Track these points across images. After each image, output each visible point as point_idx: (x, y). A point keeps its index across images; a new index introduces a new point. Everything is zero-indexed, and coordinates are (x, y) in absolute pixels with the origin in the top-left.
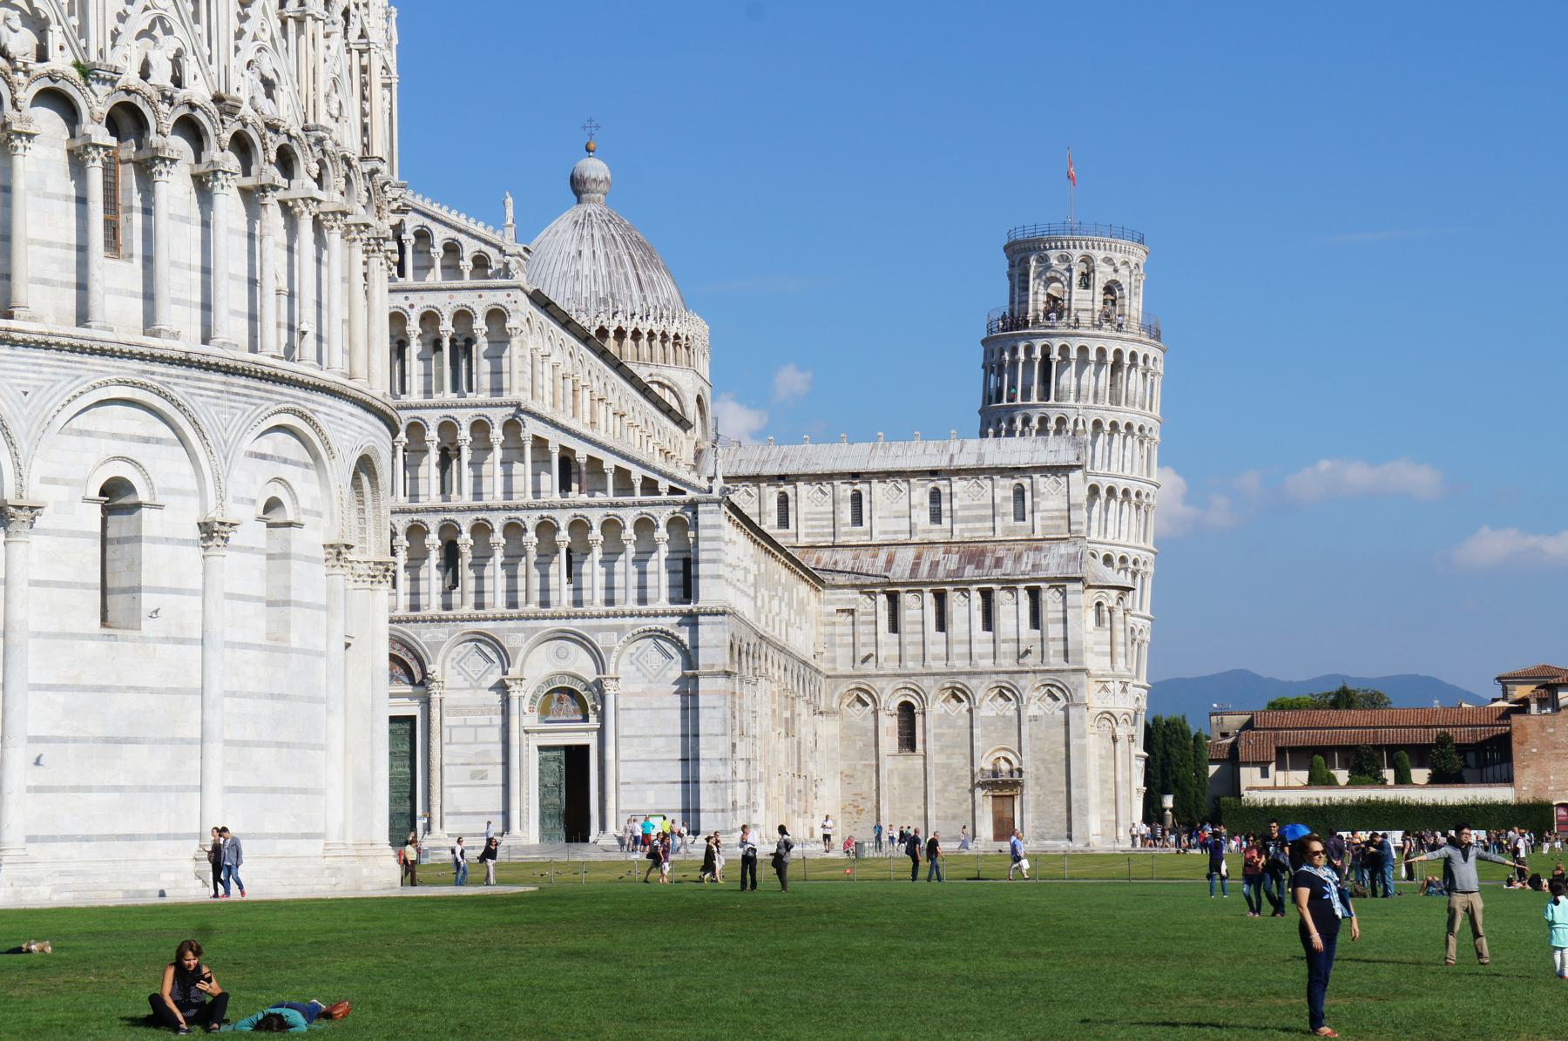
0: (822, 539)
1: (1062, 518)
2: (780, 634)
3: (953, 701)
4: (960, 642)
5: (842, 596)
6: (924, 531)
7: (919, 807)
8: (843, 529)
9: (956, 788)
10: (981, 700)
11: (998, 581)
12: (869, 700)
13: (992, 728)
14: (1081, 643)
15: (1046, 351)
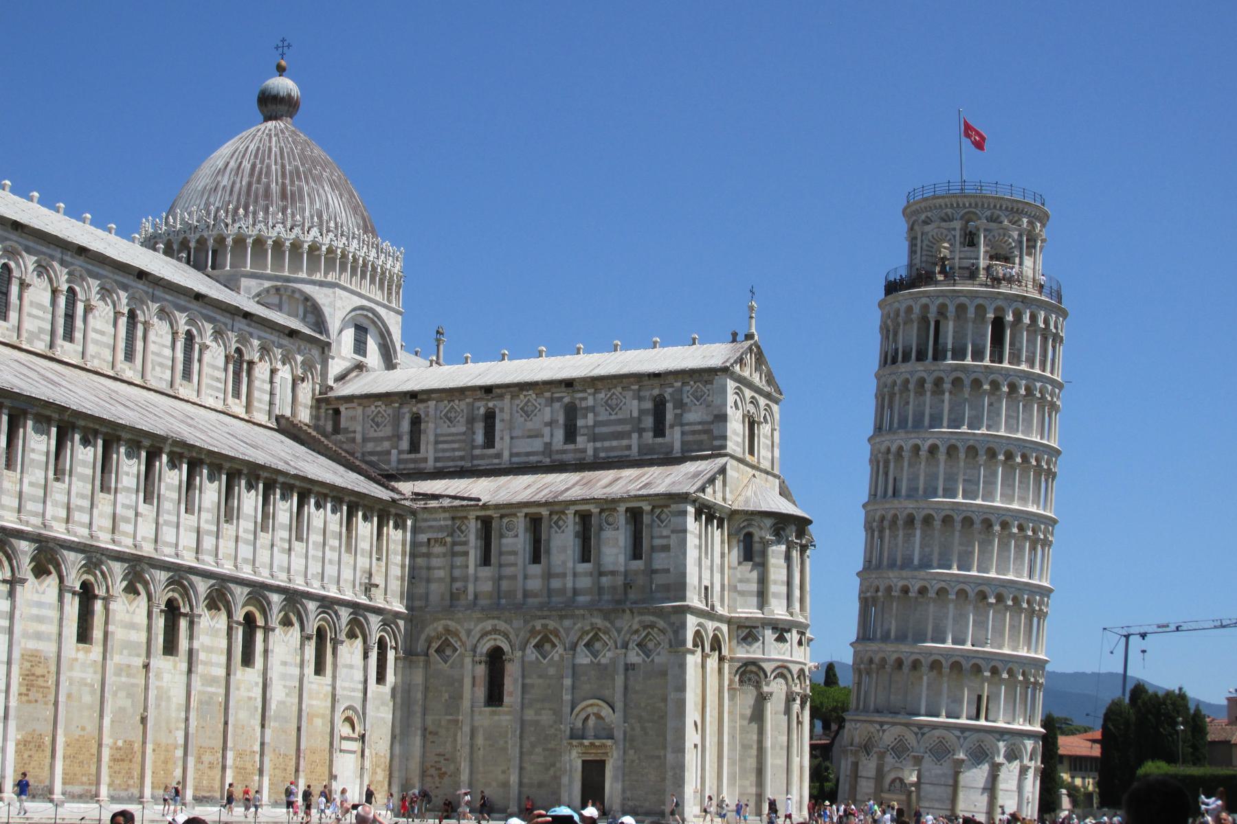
0: (451, 464)
1: (705, 432)
2: (156, 541)
3: (547, 647)
4: (558, 575)
5: (434, 523)
6: (558, 452)
7: (504, 772)
8: (477, 452)
9: (544, 750)
10: (574, 647)
11: (594, 500)
12: (457, 645)
13: (586, 678)
14: (684, 575)
15: (925, 307)
